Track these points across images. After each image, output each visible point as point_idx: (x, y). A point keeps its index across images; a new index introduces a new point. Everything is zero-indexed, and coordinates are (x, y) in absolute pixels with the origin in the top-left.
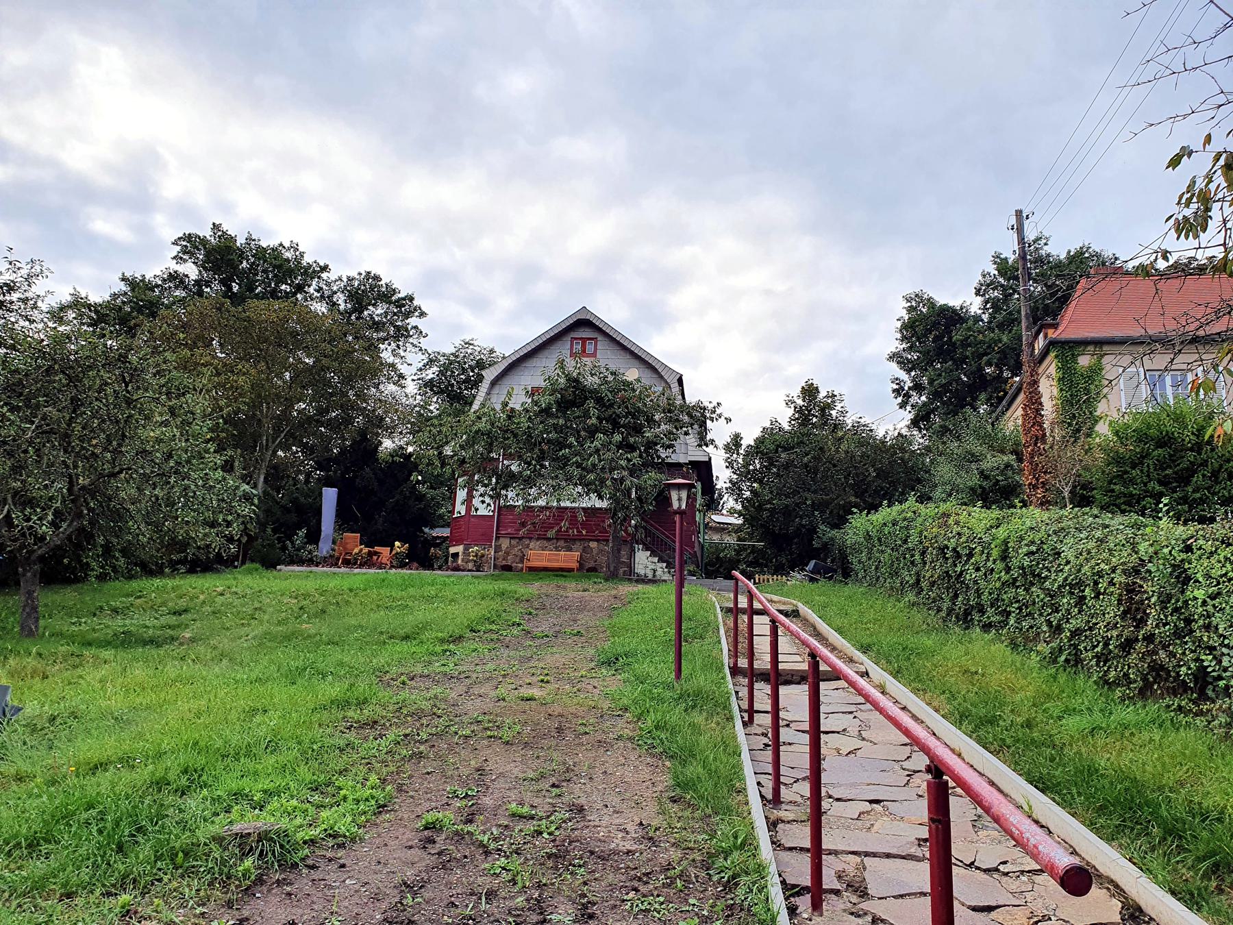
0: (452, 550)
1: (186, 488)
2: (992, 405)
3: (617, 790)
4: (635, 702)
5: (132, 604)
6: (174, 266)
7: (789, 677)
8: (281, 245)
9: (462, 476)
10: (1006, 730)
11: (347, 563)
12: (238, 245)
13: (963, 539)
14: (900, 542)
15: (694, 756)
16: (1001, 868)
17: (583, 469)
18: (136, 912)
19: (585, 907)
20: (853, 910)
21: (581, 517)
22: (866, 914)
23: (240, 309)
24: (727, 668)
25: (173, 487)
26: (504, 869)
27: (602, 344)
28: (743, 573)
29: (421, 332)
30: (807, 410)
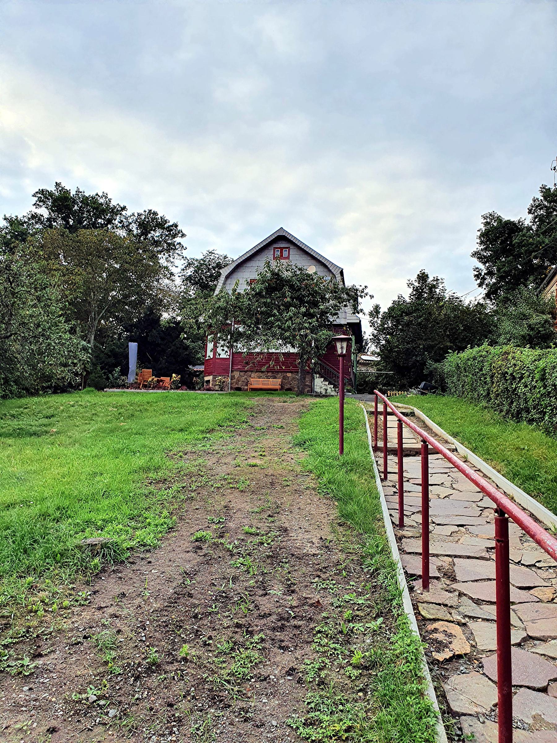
0: (206, 379)
1: (49, 344)
2: (537, 283)
3: (307, 519)
4: (316, 467)
5: (22, 412)
6: (34, 210)
7: (408, 453)
8: (97, 194)
9: (210, 335)
10: (542, 483)
11: (145, 387)
12: (72, 195)
13: (517, 368)
14: (478, 370)
15: (352, 499)
16: (537, 564)
17: (283, 329)
18: (36, 587)
19: (289, 586)
20: (447, 589)
21: (282, 358)
22: (455, 591)
23: (75, 235)
24: (371, 447)
25: (41, 344)
26: (242, 564)
27: (293, 252)
28: (380, 390)
29: (183, 246)
30: (420, 289)
